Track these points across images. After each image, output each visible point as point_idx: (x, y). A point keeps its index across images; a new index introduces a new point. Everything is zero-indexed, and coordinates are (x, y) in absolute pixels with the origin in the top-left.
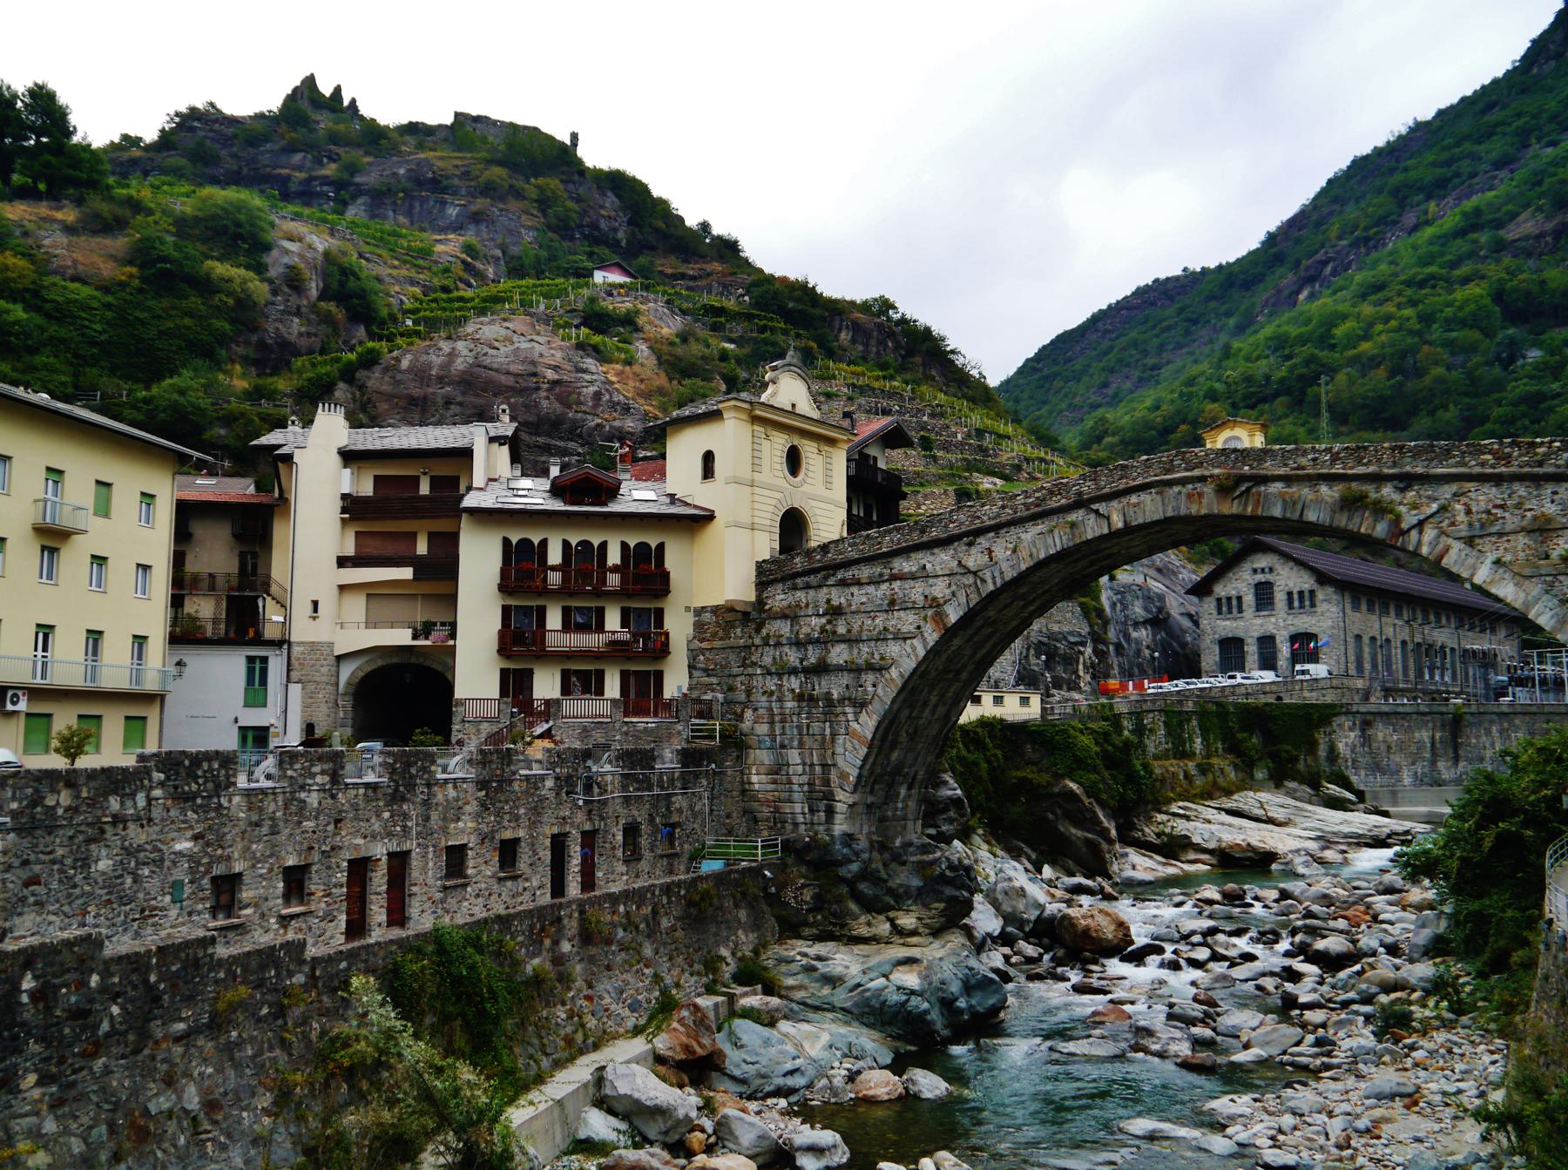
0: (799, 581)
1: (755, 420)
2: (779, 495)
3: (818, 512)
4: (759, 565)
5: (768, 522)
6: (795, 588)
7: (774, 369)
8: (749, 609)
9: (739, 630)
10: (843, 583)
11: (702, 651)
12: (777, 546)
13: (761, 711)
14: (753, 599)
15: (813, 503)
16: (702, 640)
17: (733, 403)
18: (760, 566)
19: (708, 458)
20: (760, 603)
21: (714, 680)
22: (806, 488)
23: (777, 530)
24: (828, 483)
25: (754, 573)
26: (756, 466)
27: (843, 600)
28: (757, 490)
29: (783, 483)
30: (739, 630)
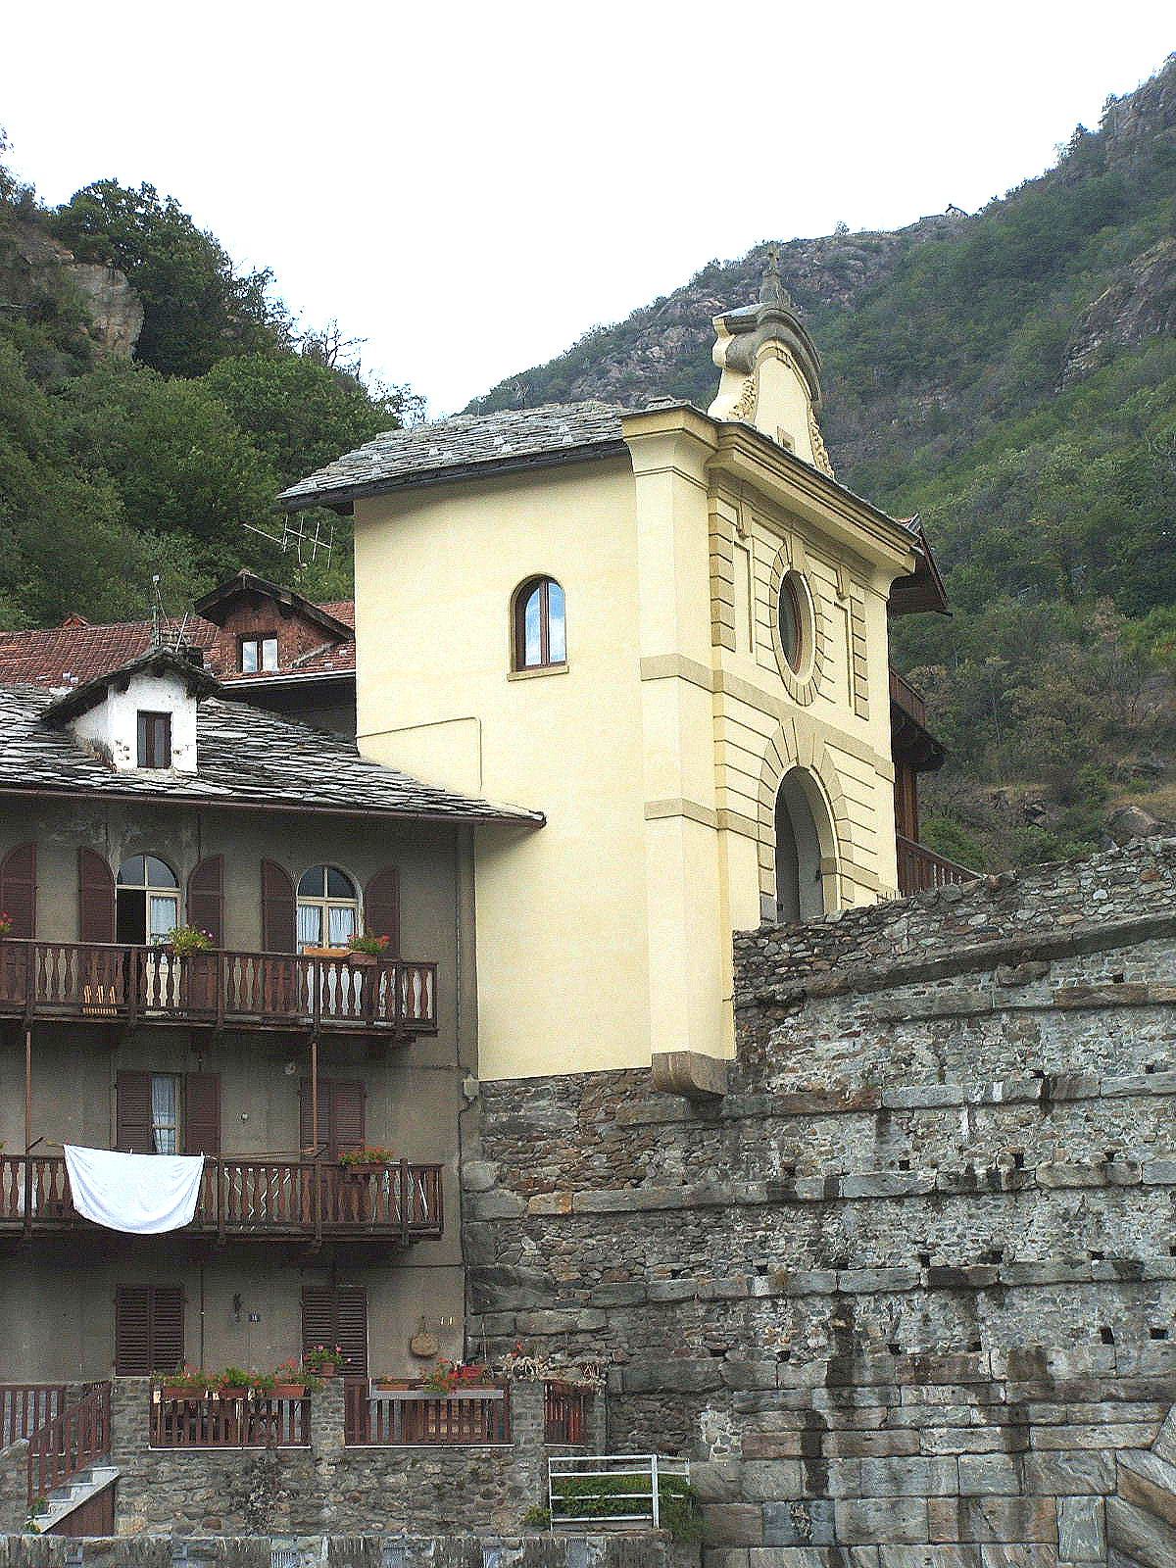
0: (905, 993)
1: (719, 480)
2: (770, 727)
3: (848, 786)
4: (738, 936)
5: (751, 810)
6: (892, 1022)
7: (738, 328)
8: (719, 1087)
9: (672, 1158)
10: (1079, 1004)
11: (532, 1226)
12: (771, 886)
13: (772, 1419)
14: (730, 1053)
15: (836, 756)
16: (531, 1188)
17: (679, 421)
18: (748, 953)
19: (533, 586)
20: (753, 1061)
21: (584, 1319)
22: (818, 710)
23: (771, 836)
24: (858, 696)
25: (730, 971)
26: (720, 632)
27: (1078, 1056)
28: (732, 707)
29: (772, 686)
30: (672, 1158)
